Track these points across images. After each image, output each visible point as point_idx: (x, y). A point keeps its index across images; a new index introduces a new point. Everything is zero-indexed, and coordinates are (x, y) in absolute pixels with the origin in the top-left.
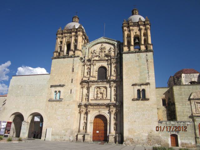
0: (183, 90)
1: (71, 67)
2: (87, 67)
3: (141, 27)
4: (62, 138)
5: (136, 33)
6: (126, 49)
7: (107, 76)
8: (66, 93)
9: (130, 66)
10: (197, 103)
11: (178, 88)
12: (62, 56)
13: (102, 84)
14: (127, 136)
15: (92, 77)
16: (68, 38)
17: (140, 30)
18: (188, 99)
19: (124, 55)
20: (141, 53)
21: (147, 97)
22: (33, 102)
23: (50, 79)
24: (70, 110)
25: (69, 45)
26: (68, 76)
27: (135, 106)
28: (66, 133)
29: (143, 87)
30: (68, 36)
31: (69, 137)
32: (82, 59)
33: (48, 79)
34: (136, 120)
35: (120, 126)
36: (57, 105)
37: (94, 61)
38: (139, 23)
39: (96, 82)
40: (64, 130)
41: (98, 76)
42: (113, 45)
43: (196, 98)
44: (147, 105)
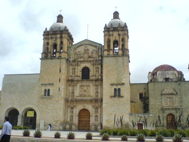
0: (156, 86)
1: (58, 67)
2: (73, 67)
3: (120, 32)
4: (54, 128)
5: (115, 38)
6: (106, 53)
7: (90, 75)
8: (55, 91)
9: (109, 68)
10: (168, 98)
11: (152, 85)
12: (49, 56)
13: (85, 83)
14: (105, 125)
15: (77, 76)
16: (55, 40)
17: (119, 35)
18: (160, 94)
19: (104, 59)
20: (119, 57)
21: (121, 94)
22: (26, 98)
23: (40, 78)
24: (59, 105)
25: (55, 46)
26: (56, 75)
27: (112, 102)
28: (57, 124)
29: (119, 87)
30: (54, 37)
31: (59, 127)
32: (67, 60)
33: (38, 78)
34: (113, 113)
35: (100, 118)
36: (48, 101)
37: (79, 62)
38: (118, 29)
39: (82, 81)
40: (55, 121)
41: (82, 75)
42: (96, 47)
43: (167, 93)
44: (122, 101)
